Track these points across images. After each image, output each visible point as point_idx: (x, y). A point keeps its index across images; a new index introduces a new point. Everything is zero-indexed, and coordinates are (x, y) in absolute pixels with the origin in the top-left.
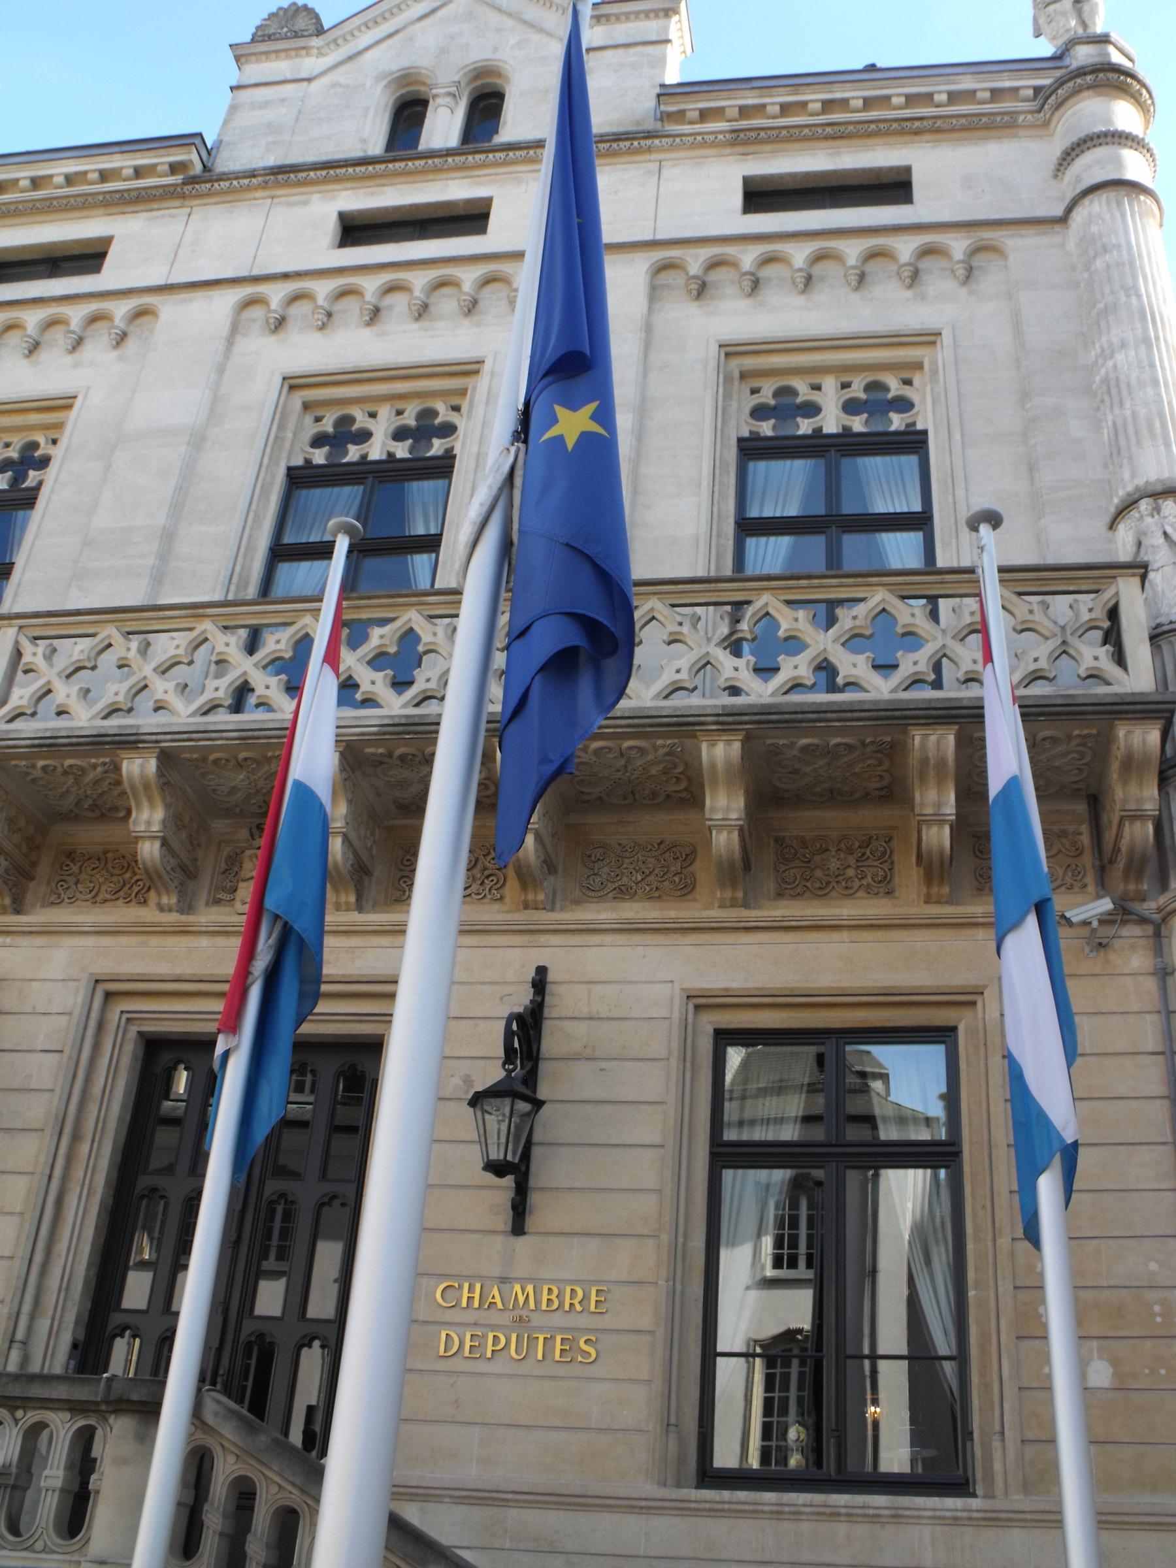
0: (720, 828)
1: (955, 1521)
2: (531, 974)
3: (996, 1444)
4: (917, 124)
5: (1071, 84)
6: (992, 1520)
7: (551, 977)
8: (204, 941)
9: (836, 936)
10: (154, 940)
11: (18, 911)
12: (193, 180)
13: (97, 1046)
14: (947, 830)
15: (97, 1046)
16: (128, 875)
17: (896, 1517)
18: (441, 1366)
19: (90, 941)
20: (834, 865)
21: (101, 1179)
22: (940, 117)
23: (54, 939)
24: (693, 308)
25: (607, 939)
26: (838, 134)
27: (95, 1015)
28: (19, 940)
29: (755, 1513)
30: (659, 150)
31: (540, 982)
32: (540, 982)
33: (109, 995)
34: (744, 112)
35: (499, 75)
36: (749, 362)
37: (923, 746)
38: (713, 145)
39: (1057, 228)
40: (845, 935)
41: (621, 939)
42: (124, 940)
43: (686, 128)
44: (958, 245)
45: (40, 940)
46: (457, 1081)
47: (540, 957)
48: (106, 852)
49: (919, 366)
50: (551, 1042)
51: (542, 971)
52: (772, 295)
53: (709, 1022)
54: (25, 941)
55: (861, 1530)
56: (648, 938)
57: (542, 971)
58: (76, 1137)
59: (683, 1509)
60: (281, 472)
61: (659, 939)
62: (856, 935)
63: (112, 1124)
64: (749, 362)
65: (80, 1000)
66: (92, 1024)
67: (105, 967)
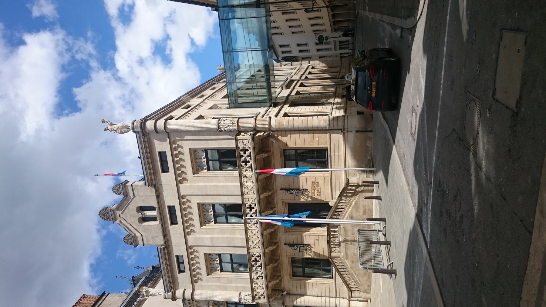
2: (281, 190)
7: (281, 188)
12: (166, 246)
13: (291, 231)
14: (266, 154)
15: (291, 231)
21: (305, 228)
31: (282, 189)
32: (282, 189)
33: (286, 231)
35: (138, 207)
39: (169, 133)
47: (279, 190)
50: (288, 188)
51: (280, 189)
57: (280, 189)
58: (301, 232)
60: (215, 224)
63: (299, 228)
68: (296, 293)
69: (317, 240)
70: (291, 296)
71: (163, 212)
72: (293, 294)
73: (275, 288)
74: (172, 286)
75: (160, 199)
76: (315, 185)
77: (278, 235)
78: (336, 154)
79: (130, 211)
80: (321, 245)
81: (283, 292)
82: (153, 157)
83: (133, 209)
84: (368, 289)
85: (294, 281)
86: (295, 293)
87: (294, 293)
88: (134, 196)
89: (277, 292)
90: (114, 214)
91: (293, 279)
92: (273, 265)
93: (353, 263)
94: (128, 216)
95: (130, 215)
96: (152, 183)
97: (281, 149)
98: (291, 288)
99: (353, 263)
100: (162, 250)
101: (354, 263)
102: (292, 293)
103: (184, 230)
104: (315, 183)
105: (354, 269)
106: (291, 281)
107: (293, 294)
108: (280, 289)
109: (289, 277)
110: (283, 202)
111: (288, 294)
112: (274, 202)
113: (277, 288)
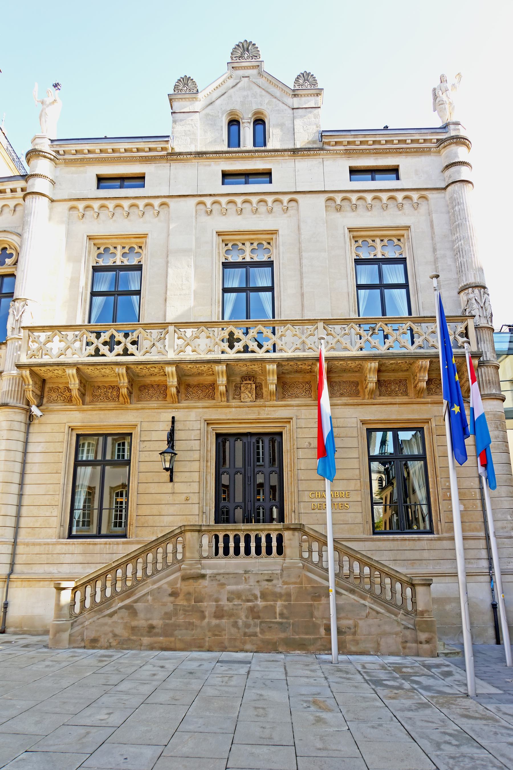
0: (371, 382)
1: (431, 540)
3: (439, 523)
4: (401, 150)
5: (449, 141)
6: (439, 539)
8: (234, 409)
9: (395, 406)
10: (219, 409)
11: (179, 403)
14: (425, 383)
16: (207, 391)
17: (419, 540)
18: (313, 511)
19: (201, 410)
20: (393, 387)
22: (408, 148)
23: (190, 410)
24: (338, 215)
25: (340, 407)
26: (377, 152)
27: (206, 429)
28: (180, 410)
29: (388, 540)
30: (323, 155)
34: (349, 143)
36: (355, 234)
37: (422, 364)
38: (339, 154)
39: (443, 191)
40: (397, 405)
41: (343, 407)
42: (211, 409)
43: (331, 148)
44: (415, 196)
45: (186, 410)
46: (307, 443)
48: (199, 384)
49: (403, 236)
52: (361, 210)
53: (365, 428)
54: (182, 410)
55: (411, 542)
56: (350, 407)
58: (207, 461)
59: (373, 540)
61: (352, 407)
62: (400, 406)
64: (355, 234)
65: (202, 426)
66: (206, 432)
67: (207, 417)
68: (30, 440)
69: (187, 500)
70: (23, 427)
71: (256, 157)
72: (27, 433)
73: (46, 389)
74: (67, 157)
75: (289, 156)
76: (339, 499)
77: (200, 404)
78: (426, 555)
79: (256, 98)
80: (172, 509)
81: (38, 406)
82: (386, 153)
83: (261, 104)
84: (83, 640)
85: (66, 437)
86: (32, 438)
87: (30, 435)
88: (293, 109)
89: (39, 393)
90: (250, 67)
91: (71, 436)
92: (125, 384)
93: (171, 595)
94: (245, 93)
95: (248, 96)
96: (328, 143)
97: (427, 421)
98: (48, 428)
99: (171, 595)
100: (162, 146)
101: (172, 599)
102: (31, 430)
103: (210, 195)
104: (345, 499)
105: (150, 598)
106: (67, 428)
107: (27, 433)
108: (45, 400)
109: (79, 424)
110: (288, 420)
111: (31, 417)
112: (289, 399)
113: (46, 394)
